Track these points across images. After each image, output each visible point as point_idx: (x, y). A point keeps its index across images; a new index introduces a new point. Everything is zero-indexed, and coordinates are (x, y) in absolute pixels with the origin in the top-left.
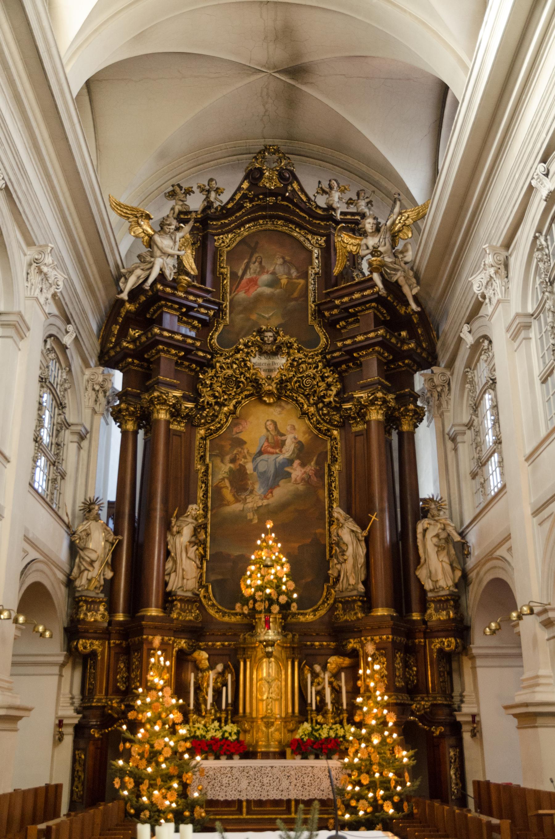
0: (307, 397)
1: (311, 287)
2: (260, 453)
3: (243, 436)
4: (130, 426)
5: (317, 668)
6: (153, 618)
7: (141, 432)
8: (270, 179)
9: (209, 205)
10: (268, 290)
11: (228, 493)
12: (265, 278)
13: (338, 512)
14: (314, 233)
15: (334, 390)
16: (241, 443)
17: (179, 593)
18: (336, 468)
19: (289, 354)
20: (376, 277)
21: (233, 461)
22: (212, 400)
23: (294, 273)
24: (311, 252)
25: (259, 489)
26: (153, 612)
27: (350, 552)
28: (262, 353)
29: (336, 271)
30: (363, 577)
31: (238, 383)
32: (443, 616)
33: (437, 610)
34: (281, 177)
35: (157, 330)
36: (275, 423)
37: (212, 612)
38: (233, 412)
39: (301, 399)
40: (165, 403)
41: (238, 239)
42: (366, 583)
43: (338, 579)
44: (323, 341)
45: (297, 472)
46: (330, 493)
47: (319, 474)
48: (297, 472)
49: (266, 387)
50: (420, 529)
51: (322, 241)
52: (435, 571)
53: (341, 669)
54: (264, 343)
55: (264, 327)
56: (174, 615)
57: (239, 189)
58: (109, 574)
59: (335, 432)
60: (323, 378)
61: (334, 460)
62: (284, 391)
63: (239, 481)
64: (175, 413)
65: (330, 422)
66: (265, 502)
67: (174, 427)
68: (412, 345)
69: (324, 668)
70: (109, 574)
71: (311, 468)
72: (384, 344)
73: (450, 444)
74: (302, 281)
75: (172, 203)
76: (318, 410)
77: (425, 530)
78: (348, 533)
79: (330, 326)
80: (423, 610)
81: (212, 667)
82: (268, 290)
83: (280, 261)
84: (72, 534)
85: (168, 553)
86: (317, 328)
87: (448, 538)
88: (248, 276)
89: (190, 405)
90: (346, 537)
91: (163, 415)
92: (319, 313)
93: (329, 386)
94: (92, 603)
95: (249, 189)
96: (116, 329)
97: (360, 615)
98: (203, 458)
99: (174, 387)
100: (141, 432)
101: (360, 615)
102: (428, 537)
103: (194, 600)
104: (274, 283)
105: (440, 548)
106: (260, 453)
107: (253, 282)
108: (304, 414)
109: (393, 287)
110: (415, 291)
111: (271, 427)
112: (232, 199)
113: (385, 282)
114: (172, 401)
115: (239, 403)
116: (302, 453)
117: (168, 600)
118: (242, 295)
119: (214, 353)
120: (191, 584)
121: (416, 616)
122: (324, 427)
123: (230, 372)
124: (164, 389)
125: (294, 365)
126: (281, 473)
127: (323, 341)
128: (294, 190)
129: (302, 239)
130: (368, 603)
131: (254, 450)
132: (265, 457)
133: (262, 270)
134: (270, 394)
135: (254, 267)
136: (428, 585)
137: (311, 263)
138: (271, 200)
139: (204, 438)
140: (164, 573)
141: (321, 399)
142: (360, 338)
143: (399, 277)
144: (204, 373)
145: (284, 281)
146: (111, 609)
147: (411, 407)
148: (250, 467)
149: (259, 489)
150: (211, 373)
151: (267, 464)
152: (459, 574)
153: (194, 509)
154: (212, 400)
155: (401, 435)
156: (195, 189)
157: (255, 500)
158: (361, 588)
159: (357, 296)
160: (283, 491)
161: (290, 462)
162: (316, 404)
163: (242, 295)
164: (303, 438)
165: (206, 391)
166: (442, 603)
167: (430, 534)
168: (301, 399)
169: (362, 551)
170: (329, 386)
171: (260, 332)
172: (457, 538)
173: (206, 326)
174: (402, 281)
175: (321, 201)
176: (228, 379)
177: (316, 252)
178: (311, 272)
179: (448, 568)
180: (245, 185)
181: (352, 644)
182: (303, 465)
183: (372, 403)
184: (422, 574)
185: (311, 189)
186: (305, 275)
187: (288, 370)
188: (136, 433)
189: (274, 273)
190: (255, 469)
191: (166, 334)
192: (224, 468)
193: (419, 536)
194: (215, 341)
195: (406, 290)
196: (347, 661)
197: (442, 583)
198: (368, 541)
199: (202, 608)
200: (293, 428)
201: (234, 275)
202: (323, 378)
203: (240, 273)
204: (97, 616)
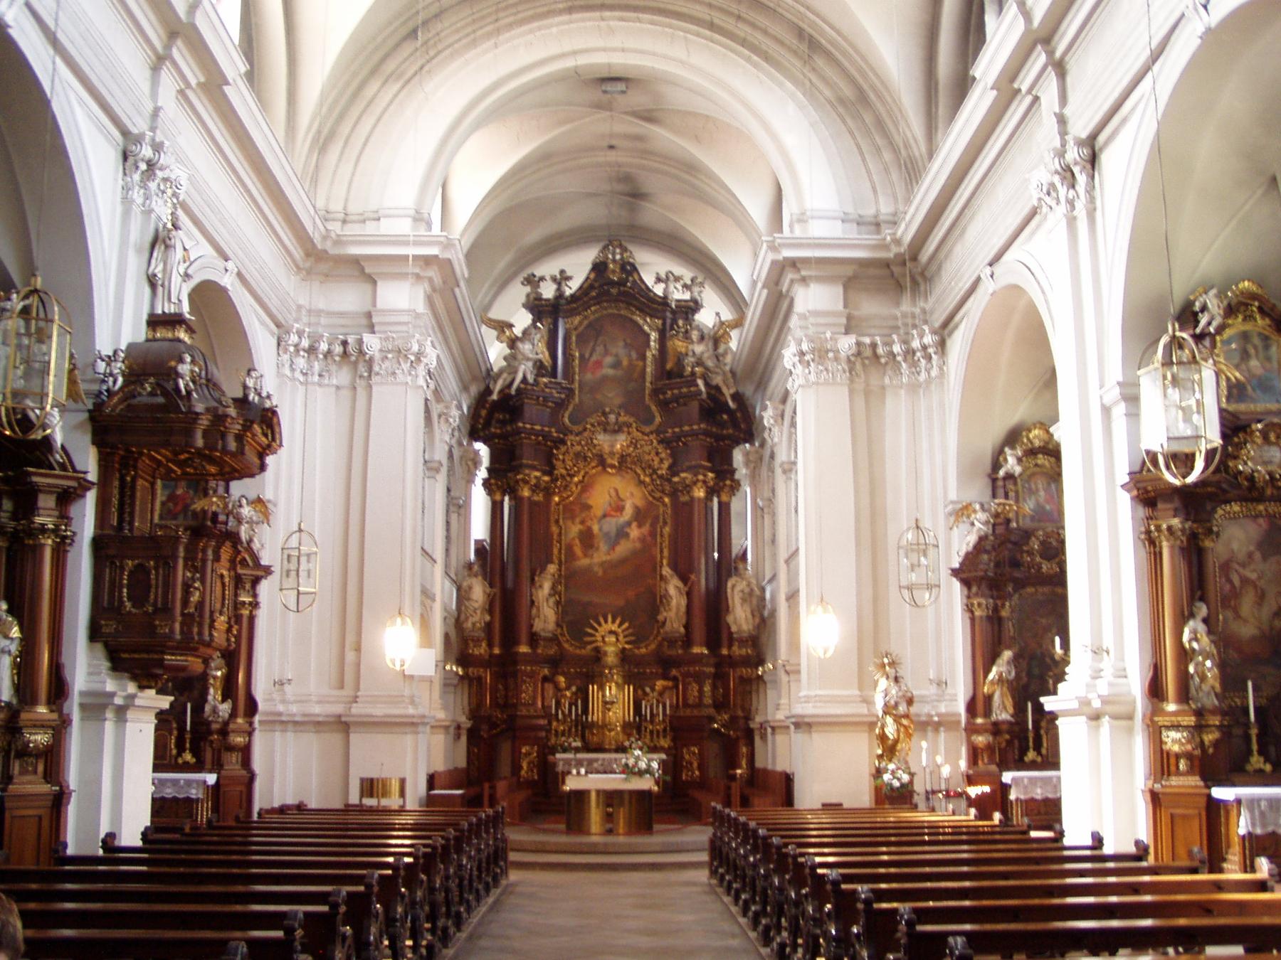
0: (644, 469)
1: (649, 370)
2: (605, 516)
3: (590, 502)
4: (498, 497)
5: (648, 690)
6: (525, 654)
7: (507, 498)
8: (614, 272)
9: (560, 295)
10: (610, 372)
11: (578, 550)
12: (609, 360)
13: (666, 571)
14: (651, 316)
15: (666, 465)
16: (588, 507)
17: (543, 634)
18: (667, 530)
19: (629, 433)
20: (700, 382)
21: (582, 522)
22: (564, 472)
23: (634, 355)
24: (648, 335)
25: (603, 547)
26: (524, 649)
27: (674, 602)
28: (605, 431)
29: (669, 366)
30: (684, 621)
31: (585, 458)
32: (743, 652)
33: (740, 648)
34: (623, 268)
35: (521, 425)
36: (616, 491)
37: (566, 646)
38: (580, 482)
39: (639, 471)
40: (526, 482)
41: (586, 322)
42: (686, 627)
43: (664, 623)
44: (658, 419)
45: (635, 532)
46: (662, 552)
47: (653, 534)
48: (635, 532)
49: (609, 461)
50: (729, 584)
51: (659, 322)
52: (740, 617)
53: (665, 688)
54: (608, 423)
55: (607, 410)
56: (539, 651)
57: (587, 278)
58: (488, 618)
59: (666, 500)
60: (657, 454)
61: (665, 523)
62: (624, 463)
63: (587, 539)
64: (535, 488)
65: (663, 492)
66: (609, 558)
67: (536, 498)
68: (731, 431)
69: (653, 689)
70: (488, 618)
71: (646, 529)
72: (707, 433)
73: (759, 512)
74: (641, 363)
75: (528, 289)
76: (652, 480)
77: (733, 586)
78: (674, 588)
79: (664, 405)
80: (730, 646)
81: (568, 688)
82: (610, 372)
83: (621, 344)
84: (459, 589)
85: (533, 602)
86: (653, 408)
87: (751, 592)
88: (594, 358)
89: (546, 478)
90: (672, 591)
91: (526, 493)
92: (656, 392)
93: (661, 461)
94: (477, 641)
95: (595, 280)
96: (484, 413)
97: (680, 652)
98: (557, 522)
99: (534, 468)
100: (507, 498)
101: (680, 652)
102: (736, 589)
103: (554, 639)
104: (617, 365)
105: (744, 600)
106: (605, 516)
107: (599, 364)
108: (642, 483)
109: (714, 391)
110: (732, 391)
111: (613, 494)
112: (581, 287)
113: (707, 384)
114: (533, 481)
115: (586, 473)
116: (639, 516)
117: (534, 639)
118: (589, 376)
119: (566, 431)
120: (551, 626)
121: (725, 652)
122: (658, 495)
123: (578, 448)
124: (527, 472)
125: (634, 444)
126: (622, 534)
127: (658, 419)
128: (634, 281)
129: (641, 322)
130: (688, 641)
131: (599, 513)
132: (608, 519)
133: (606, 353)
134: (612, 466)
135: (600, 349)
136: (734, 629)
137: (649, 346)
138: (614, 291)
139: (558, 504)
140: (530, 618)
141: (655, 471)
142: (686, 428)
143: (717, 380)
144: (558, 449)
145: (625, 363)
146: (490, 646)
147: (728, 482)
148: (596, 528)
149: (603, 547)
150: (563, 449)
151: (611, 525)
152: (757, 620)
153: (552, 568)
154: (564, 472)
155: (720, 503)
156: (548, 278)
157: (601, 555)
158: (682, 630)
159: (684, 390)
160: (623, 549)
161: (629, 524)
162: (651, 475)
163: (589, 376)
164: (640, 503)
165: (558, 464)
166: (742, 642)
167: (738, 589)
168: (639, 471)
169: (684, 602)
170: (661, 461)
171: (604, 414)
172: (757, 592)
173: (561, 405)
174: (721, 384)
175: (659, 290)
176: (577, 455)
177: (654, 336)
178: (649, 354)
179: (750, 616)
180: (592, 276)
181: (674, 672)
182: (640, 526)
183: (695, 483)
184: (730, 619)
185: (649, 280)
186: (643, 358)
187: (628, 446)
188: (502, 502)
189: (616, 355)
190: (600, 529)
191: (528, 426)
192: (574, 529)
193: (729, 590)
194: (566, 420)
195: (725, 390)
196: (670, 684)
197: (745, 627)
198: (689, 594)
199: (559, 644)
200: (632, 494)
201: (582, 356)
202: (657, 454)
203: (587, 356)
204: (481, 650)
